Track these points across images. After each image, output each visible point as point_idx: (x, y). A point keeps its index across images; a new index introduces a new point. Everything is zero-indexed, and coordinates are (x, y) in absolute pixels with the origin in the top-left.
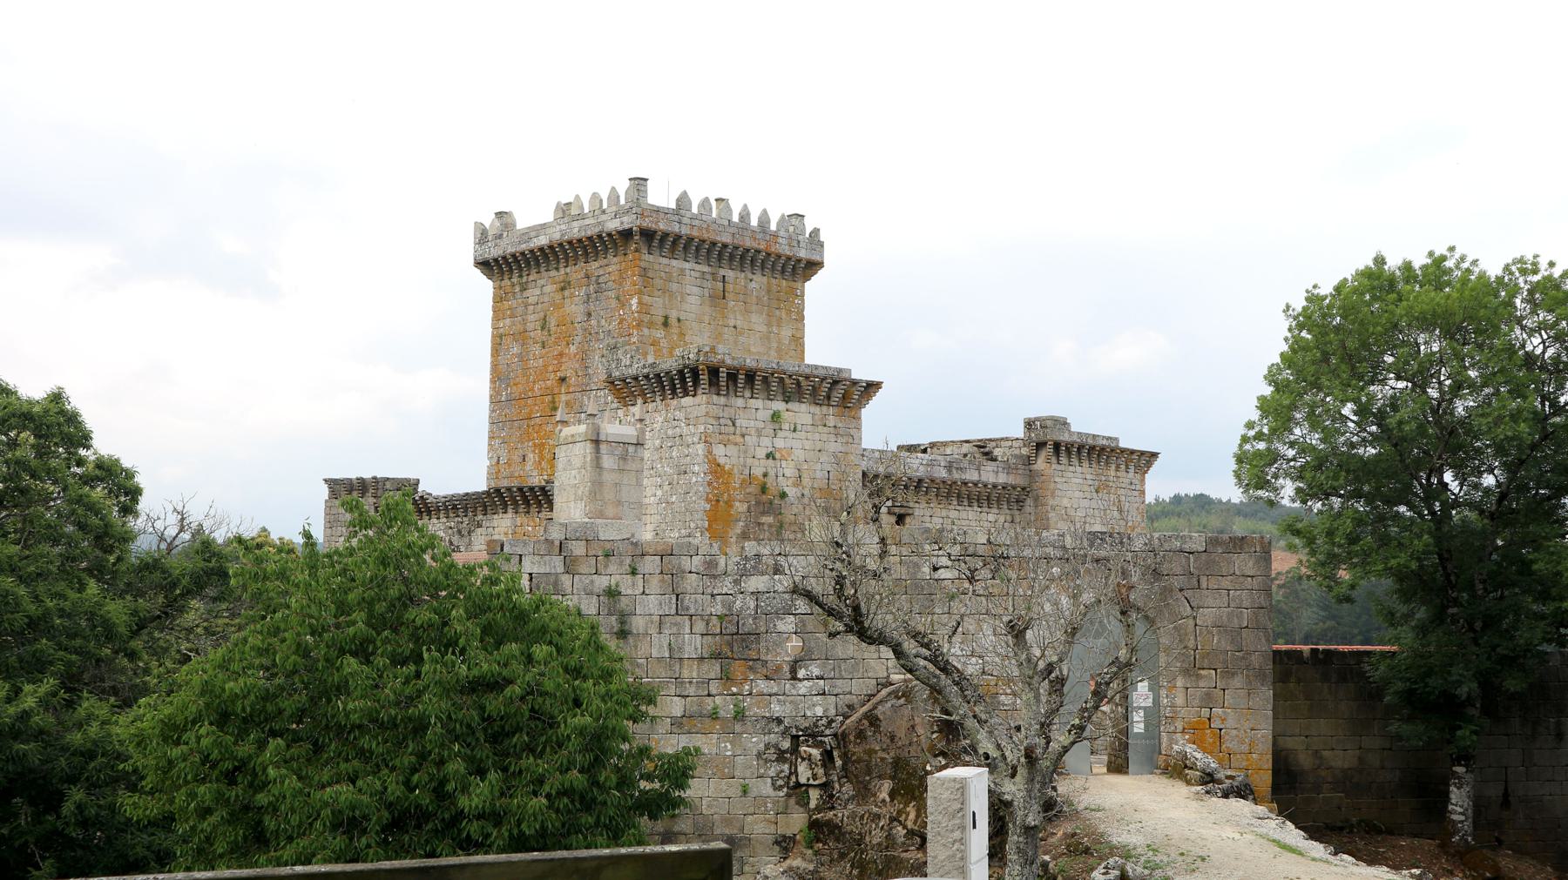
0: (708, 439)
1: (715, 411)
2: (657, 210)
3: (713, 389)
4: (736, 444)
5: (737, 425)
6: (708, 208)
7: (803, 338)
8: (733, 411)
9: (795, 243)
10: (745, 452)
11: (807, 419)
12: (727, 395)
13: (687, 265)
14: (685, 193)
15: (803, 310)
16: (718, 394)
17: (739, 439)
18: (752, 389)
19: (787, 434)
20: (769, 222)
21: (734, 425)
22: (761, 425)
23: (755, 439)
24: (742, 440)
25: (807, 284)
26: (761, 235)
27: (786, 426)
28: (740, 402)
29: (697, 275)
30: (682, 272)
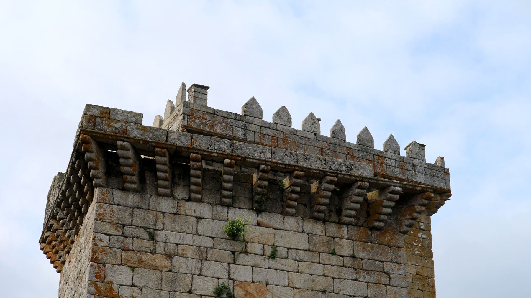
0: (99, 255)
1: (118, 214)
2: (214, 113)
3: (114, 182)
4: (155, 268)
5: (158, 239)
6: (285, 119)
7: (432, 277)
8: (151, 216)
9: (409, 167)
10: (173, 282)
11: (302, 242)
12: (141, 191)
14: (253, 99)
15: (430, 246)
16: (124, 190)
17: (161, 261)
18: (189, 184)
19: (258, 260)
20: (371, 140)
21: (152, 238)
22: (209, 243)
23: (192, 264)
24: (167, 263)
25: (433, 217)
26: (361, 153)
27: (257, 248)
28: (166, 205)
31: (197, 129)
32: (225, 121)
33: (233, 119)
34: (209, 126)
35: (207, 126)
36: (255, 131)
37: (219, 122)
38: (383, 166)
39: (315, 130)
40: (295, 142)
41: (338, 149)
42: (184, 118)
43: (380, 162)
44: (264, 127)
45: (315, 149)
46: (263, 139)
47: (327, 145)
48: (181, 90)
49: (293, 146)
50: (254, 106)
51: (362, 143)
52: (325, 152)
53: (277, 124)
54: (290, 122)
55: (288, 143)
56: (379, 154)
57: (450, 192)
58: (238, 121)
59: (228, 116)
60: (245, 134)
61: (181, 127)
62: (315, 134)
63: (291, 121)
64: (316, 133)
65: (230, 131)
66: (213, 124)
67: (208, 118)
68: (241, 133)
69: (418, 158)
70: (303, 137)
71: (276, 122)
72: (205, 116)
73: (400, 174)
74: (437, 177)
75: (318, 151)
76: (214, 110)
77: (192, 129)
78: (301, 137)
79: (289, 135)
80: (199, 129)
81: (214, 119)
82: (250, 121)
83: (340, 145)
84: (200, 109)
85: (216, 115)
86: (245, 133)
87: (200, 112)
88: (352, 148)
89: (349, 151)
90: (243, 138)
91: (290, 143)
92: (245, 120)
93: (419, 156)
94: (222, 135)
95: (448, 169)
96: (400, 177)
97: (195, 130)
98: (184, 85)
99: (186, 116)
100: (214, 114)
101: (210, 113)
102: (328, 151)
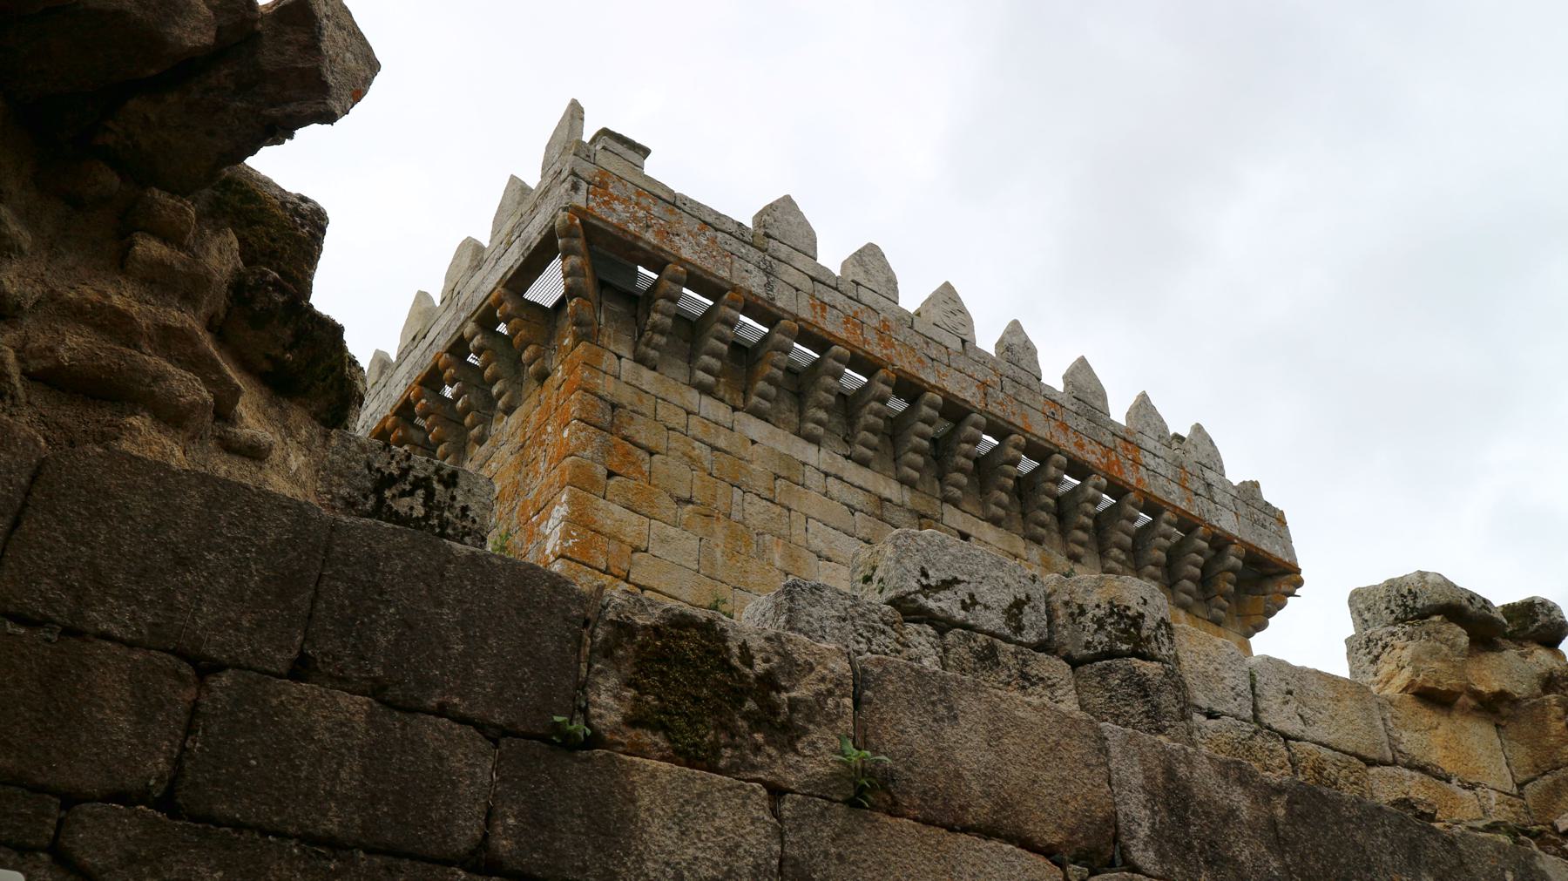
6: (882, 278)
13: (810, 453)
29: (858, 499)
30: (788, 473)
31: (620, 229)
32: (707, 233)
33: (730, 234)
34: (658, 233)
35: (650, 230)
36: (797, 286)
37: (689, 232)
38: (1138, 469)
39: (962, 330)
40: (912, 349)
41: (1026, 396)
42: (575, 187)
43: (1130, 457)
44: (824, 284)
45: (966, 381)
46: (822, 316)
47: (996, 379)
48: (568, 117)
49: (907, 357)
50: (791, 219)
51: (1081, 396)
52: (993, 397)
53: (858, 284)
54: (896, 291)
55: (893, 346)
56: (1126, 436)
57: (1298, 571)
58: (747, 246)
59: (717, 221)
60: (768, 285)
61: (565, 209)
62: (963, 341)
63: (896, 287)
64: (965, 337)
65: (725, 264)
66: (669, 230)
67: (655, 210)
68: (757, 280)
69: (1214, 468)
70: (931, 339)
71: (856, 279)
72: (644, 202)
73: (1182, 500)
74: (1263, 526)
75: (974, 389)
76: (671, 192)
77: (600, 224)
78: (928, 340)
79: (893, 325)
80: (624, 231)
81: (673, 219)
82: (783, 257)
83: (1028, 387)
84: (627, 178)
85: (679, 208)
86: (769, 283)
87: (629, 185)
88: (1060, 402)
89: (1052, 410)
90: (764, 295)
91: (898, 348)
92: (766, 250)
93: (1215, 464)
94: (700, 268)
95: (1282, 512)
96: (1182, 507)
97: (611, 230)
98: (575, 113)
99: (584, 185)
100: (674, 205)
101: (660, 198)
102: (1001, 395)
